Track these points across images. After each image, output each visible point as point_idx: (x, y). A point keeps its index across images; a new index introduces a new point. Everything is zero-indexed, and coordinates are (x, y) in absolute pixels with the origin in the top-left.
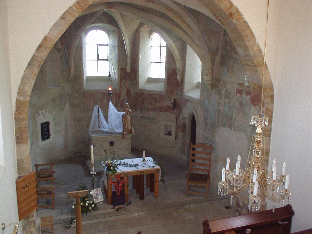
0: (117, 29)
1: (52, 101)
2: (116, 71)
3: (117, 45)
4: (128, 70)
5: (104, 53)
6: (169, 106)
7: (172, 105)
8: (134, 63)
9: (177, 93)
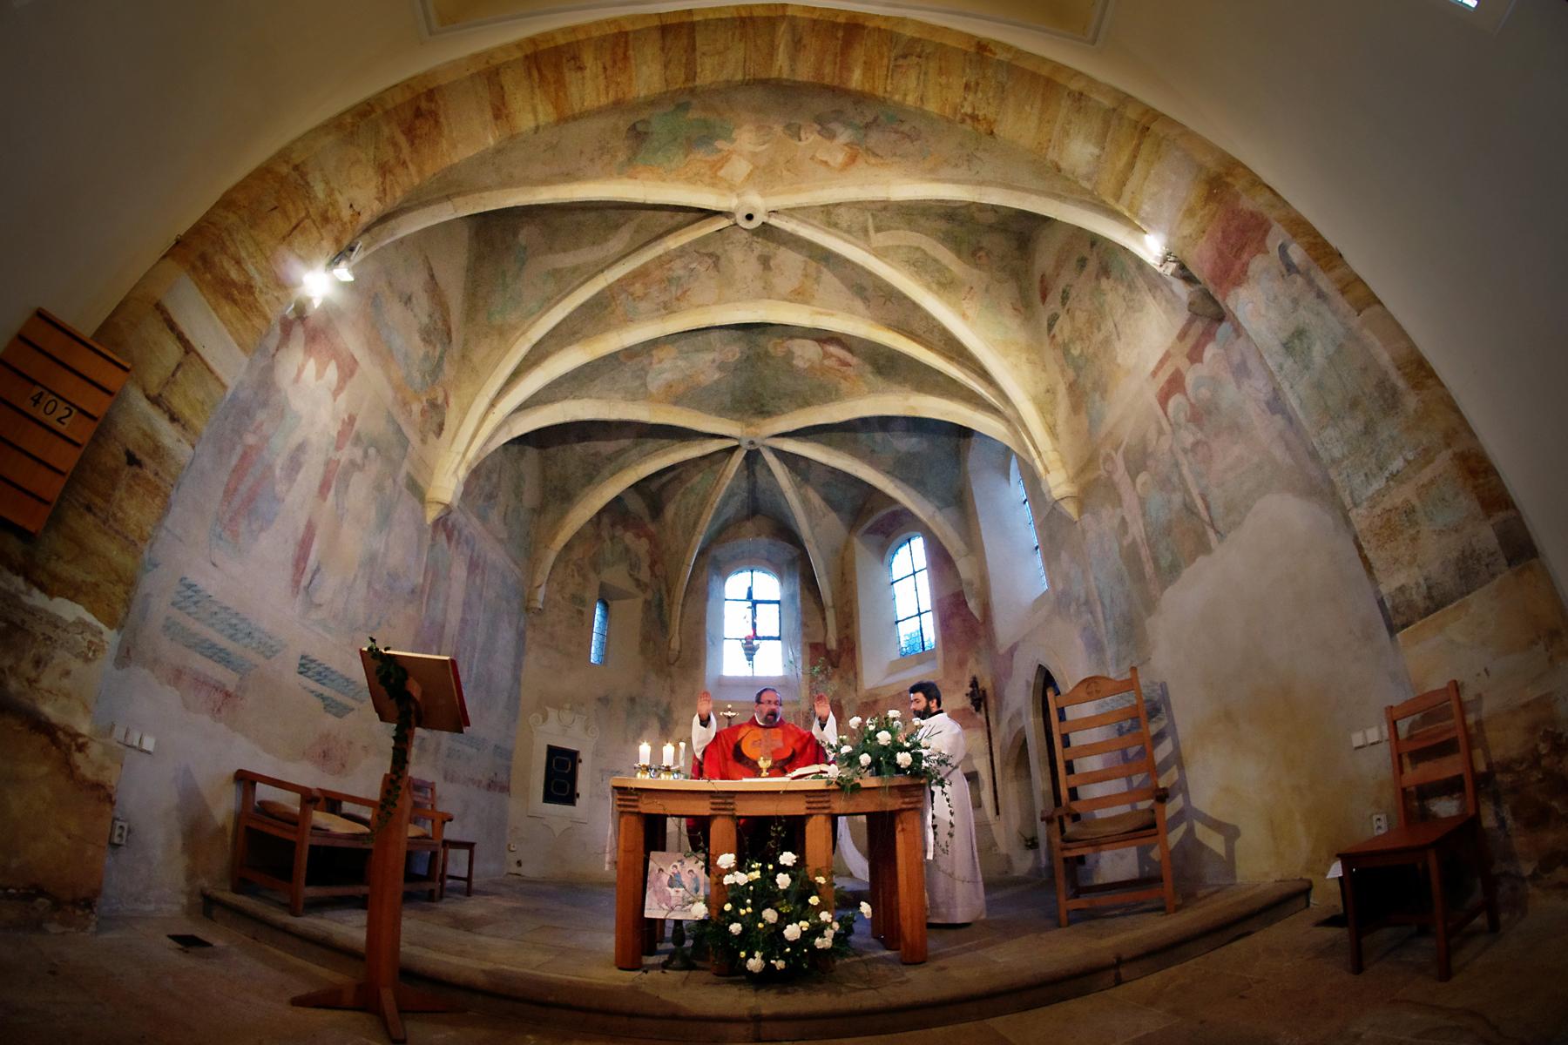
0: (797, 552)
1: (599, 699)
2: (798, 655)
3: (798, 588)
4: (833, 644)
5: (769, 620)
6: (958, 711)
7: (967, 703)
8: (847, 626)
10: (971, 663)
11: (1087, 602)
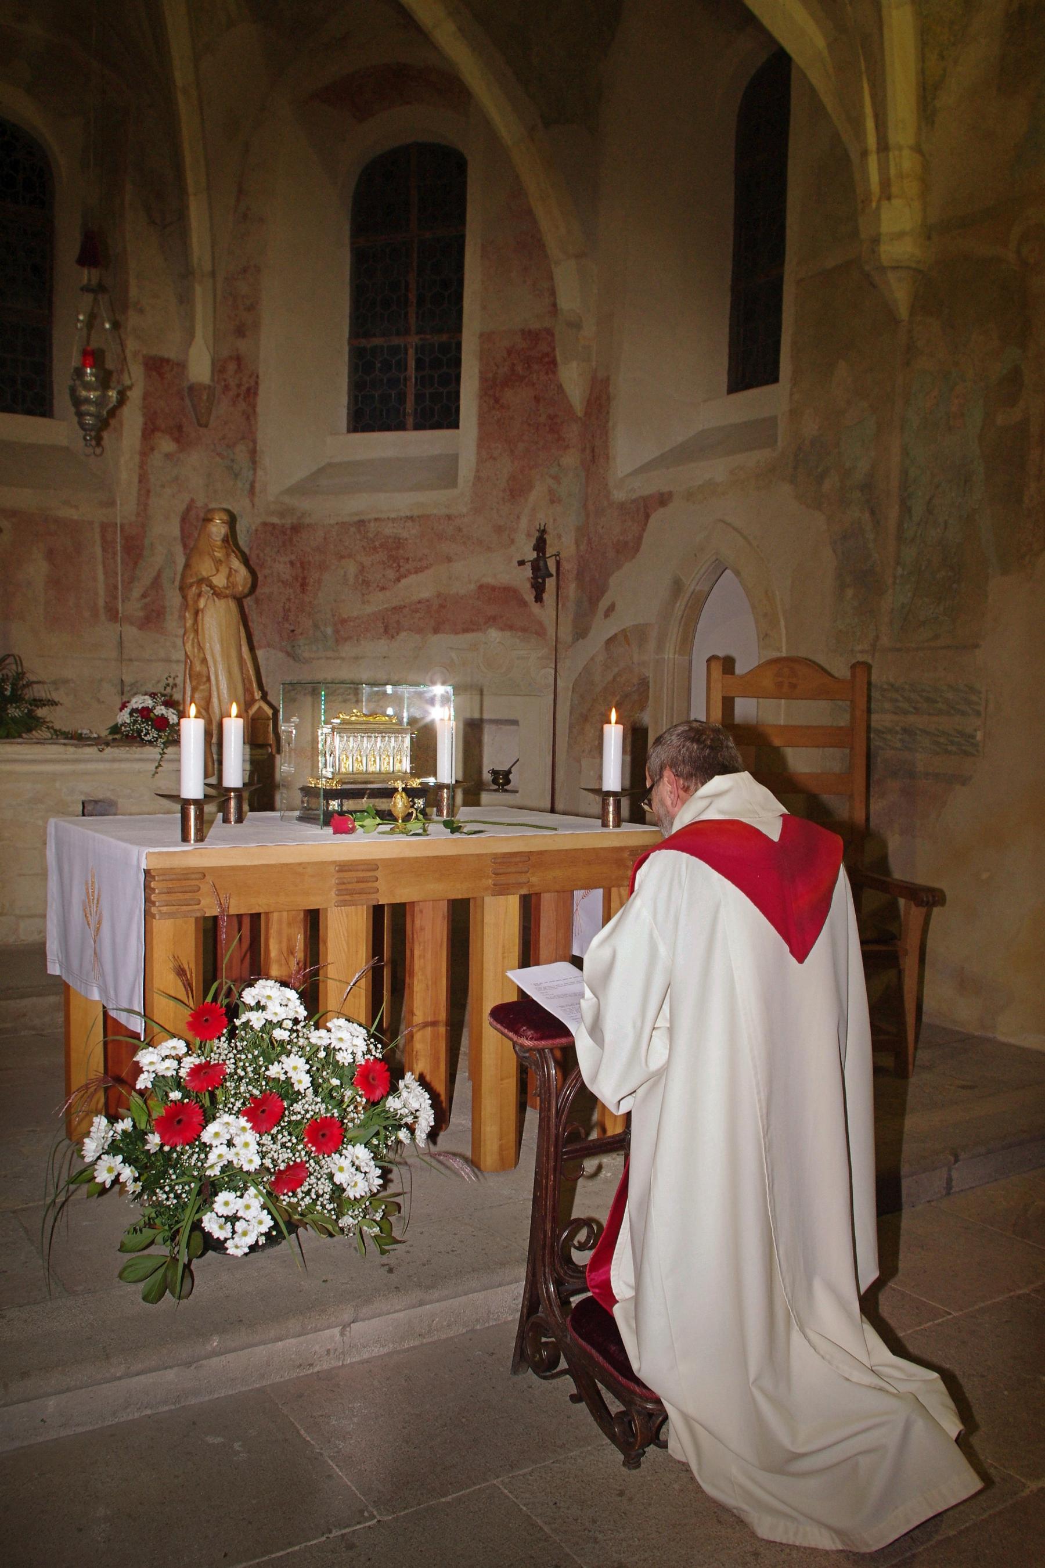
6: (493, 589)
9: (551, 491)
10: (538, 493)
11: (867, 487)
